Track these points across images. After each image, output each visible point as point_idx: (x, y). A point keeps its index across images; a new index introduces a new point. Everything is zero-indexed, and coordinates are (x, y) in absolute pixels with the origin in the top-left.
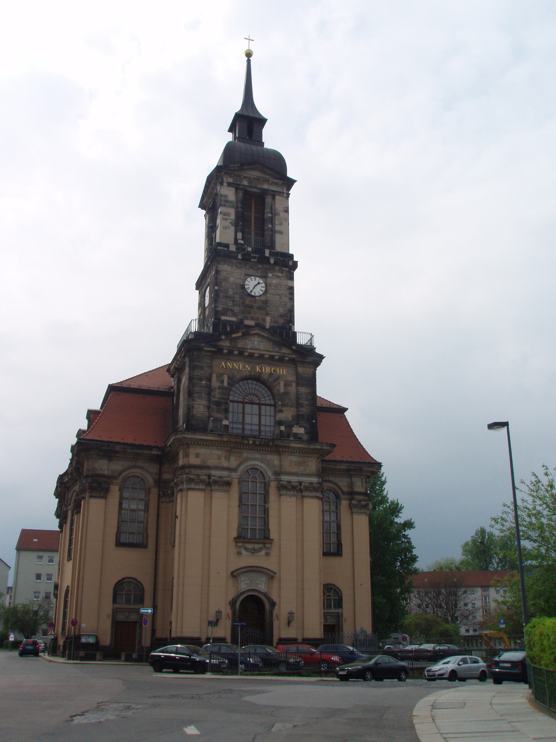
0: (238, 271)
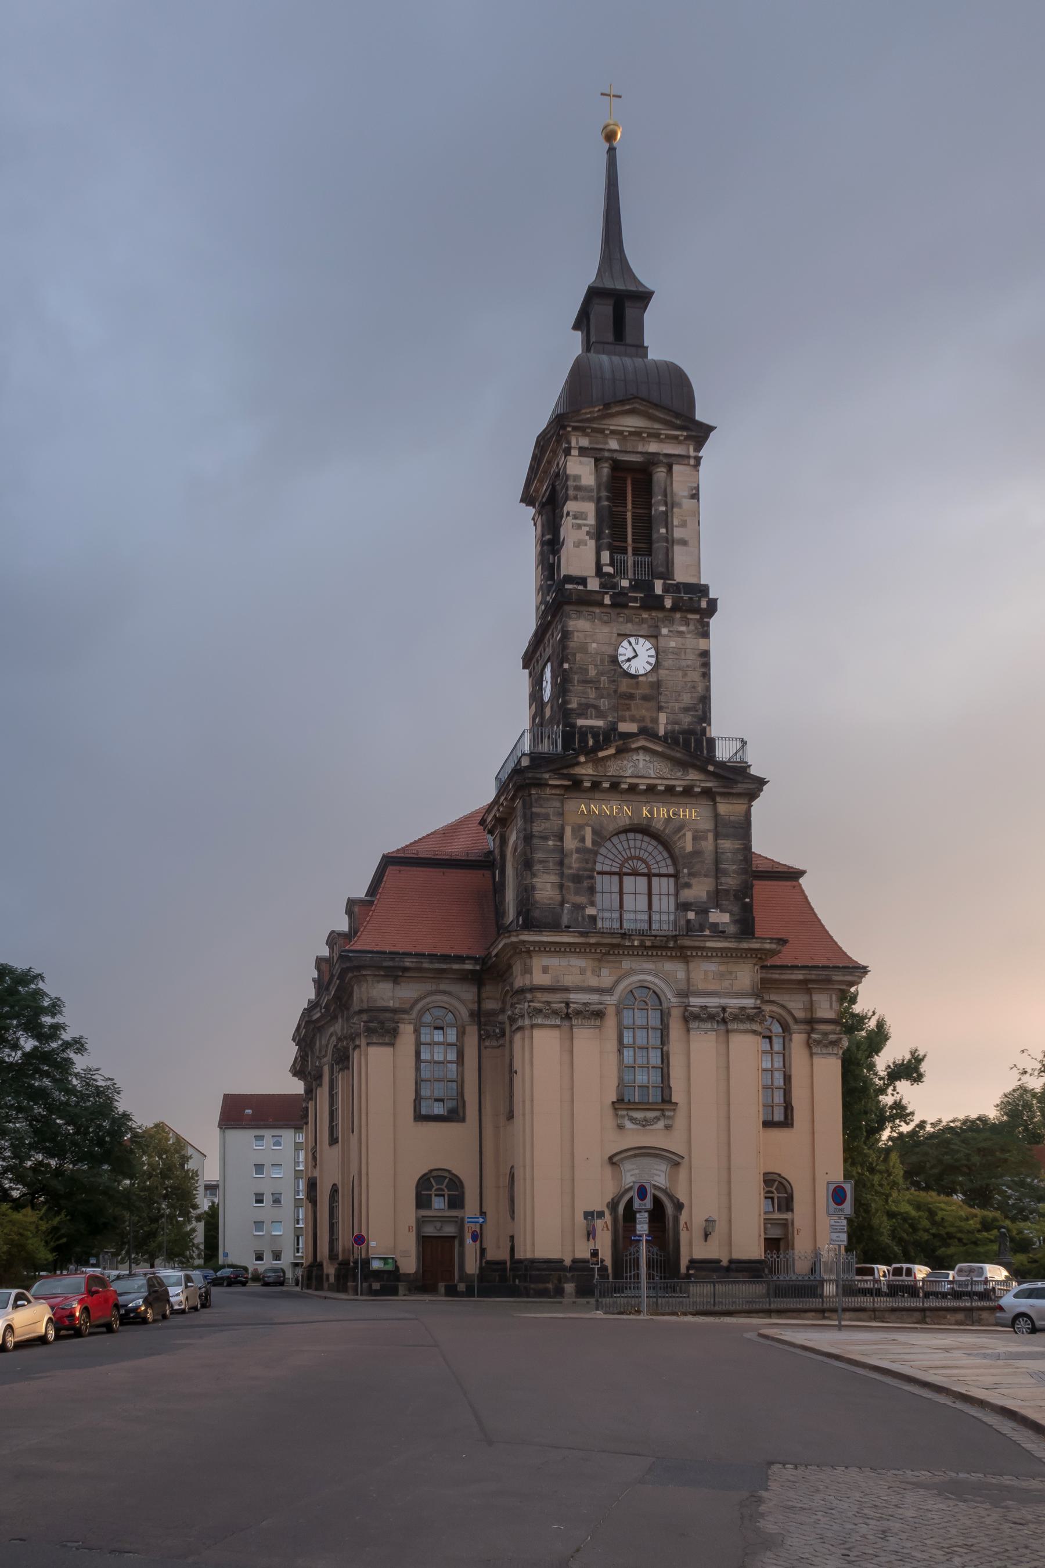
0: (606, 629)
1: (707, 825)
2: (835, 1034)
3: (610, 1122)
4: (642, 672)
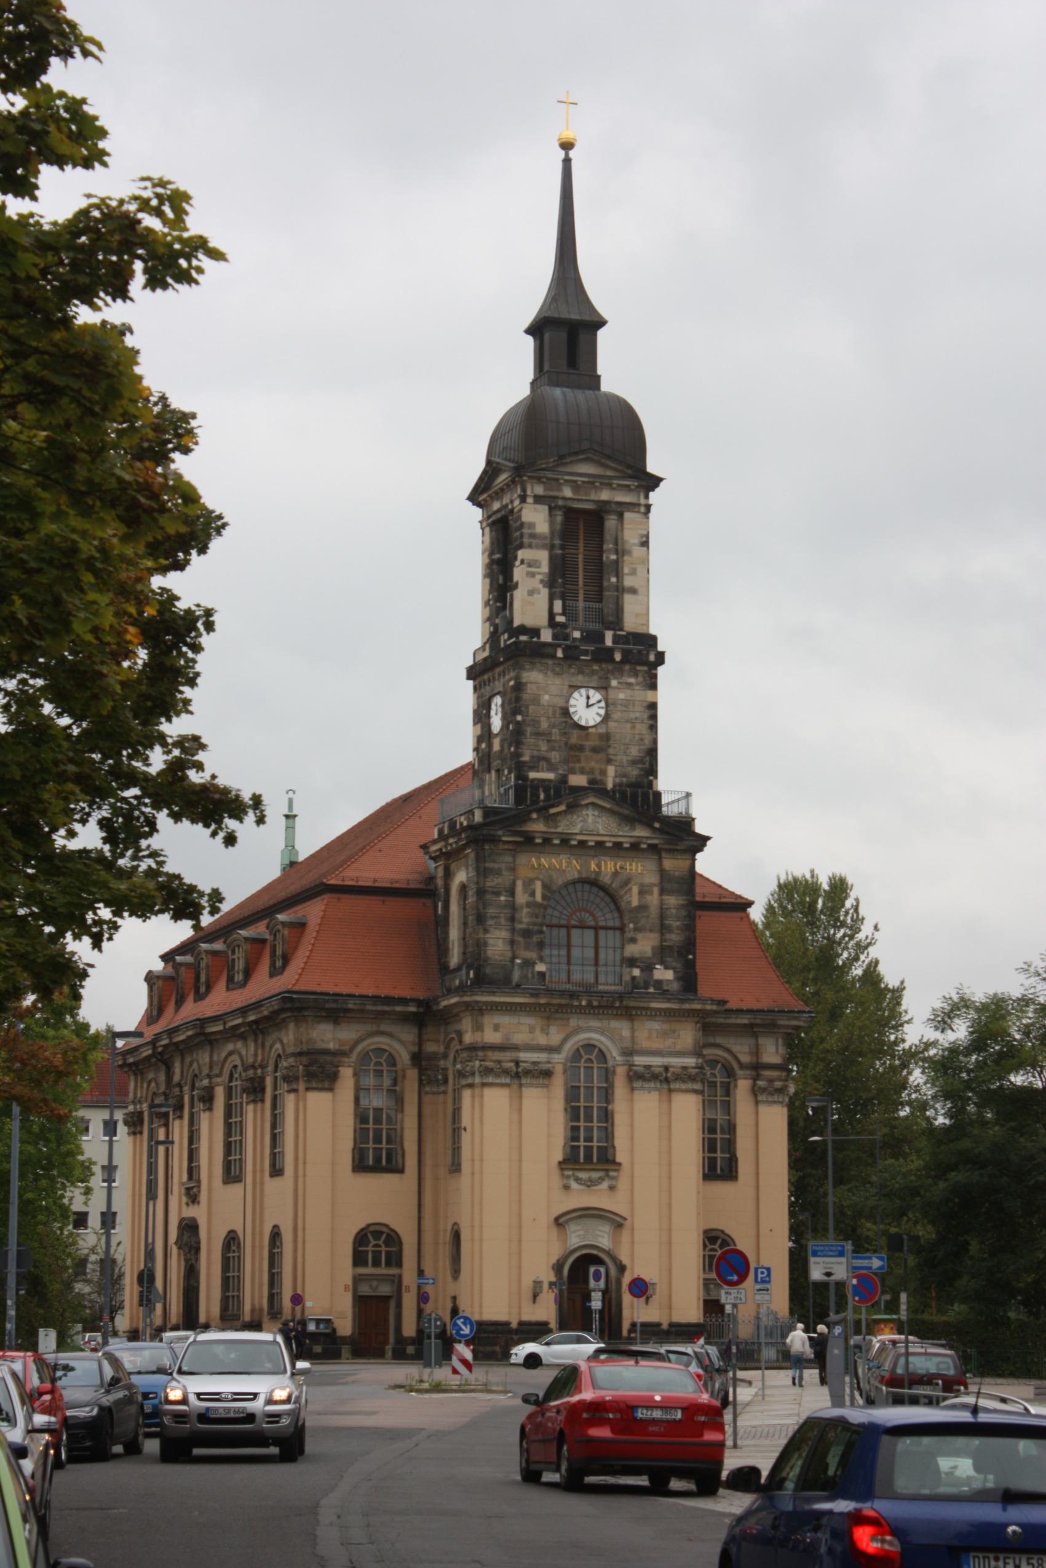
0: (558, 681)
1: (652, 878)
2: (781, 1080)
3: (557, 1182)
4: (591, 723)
